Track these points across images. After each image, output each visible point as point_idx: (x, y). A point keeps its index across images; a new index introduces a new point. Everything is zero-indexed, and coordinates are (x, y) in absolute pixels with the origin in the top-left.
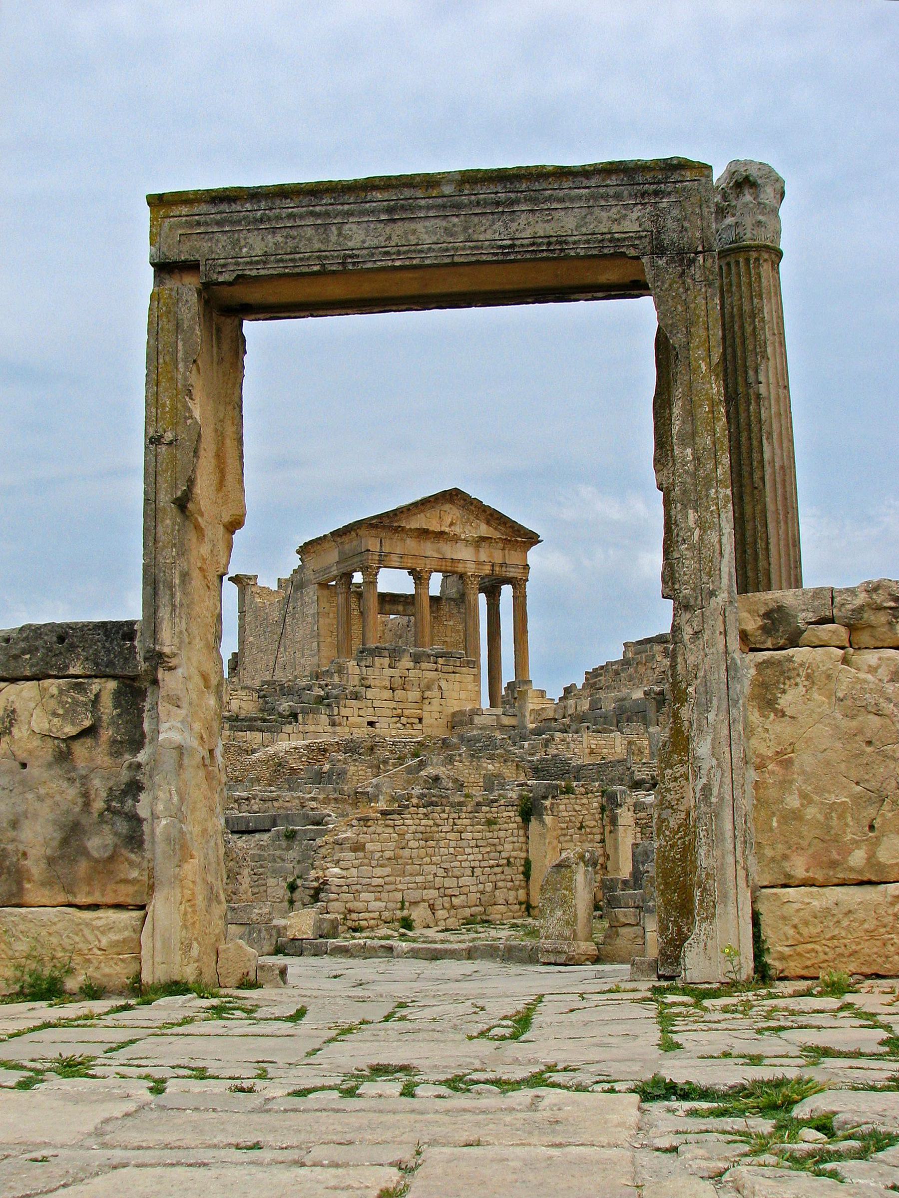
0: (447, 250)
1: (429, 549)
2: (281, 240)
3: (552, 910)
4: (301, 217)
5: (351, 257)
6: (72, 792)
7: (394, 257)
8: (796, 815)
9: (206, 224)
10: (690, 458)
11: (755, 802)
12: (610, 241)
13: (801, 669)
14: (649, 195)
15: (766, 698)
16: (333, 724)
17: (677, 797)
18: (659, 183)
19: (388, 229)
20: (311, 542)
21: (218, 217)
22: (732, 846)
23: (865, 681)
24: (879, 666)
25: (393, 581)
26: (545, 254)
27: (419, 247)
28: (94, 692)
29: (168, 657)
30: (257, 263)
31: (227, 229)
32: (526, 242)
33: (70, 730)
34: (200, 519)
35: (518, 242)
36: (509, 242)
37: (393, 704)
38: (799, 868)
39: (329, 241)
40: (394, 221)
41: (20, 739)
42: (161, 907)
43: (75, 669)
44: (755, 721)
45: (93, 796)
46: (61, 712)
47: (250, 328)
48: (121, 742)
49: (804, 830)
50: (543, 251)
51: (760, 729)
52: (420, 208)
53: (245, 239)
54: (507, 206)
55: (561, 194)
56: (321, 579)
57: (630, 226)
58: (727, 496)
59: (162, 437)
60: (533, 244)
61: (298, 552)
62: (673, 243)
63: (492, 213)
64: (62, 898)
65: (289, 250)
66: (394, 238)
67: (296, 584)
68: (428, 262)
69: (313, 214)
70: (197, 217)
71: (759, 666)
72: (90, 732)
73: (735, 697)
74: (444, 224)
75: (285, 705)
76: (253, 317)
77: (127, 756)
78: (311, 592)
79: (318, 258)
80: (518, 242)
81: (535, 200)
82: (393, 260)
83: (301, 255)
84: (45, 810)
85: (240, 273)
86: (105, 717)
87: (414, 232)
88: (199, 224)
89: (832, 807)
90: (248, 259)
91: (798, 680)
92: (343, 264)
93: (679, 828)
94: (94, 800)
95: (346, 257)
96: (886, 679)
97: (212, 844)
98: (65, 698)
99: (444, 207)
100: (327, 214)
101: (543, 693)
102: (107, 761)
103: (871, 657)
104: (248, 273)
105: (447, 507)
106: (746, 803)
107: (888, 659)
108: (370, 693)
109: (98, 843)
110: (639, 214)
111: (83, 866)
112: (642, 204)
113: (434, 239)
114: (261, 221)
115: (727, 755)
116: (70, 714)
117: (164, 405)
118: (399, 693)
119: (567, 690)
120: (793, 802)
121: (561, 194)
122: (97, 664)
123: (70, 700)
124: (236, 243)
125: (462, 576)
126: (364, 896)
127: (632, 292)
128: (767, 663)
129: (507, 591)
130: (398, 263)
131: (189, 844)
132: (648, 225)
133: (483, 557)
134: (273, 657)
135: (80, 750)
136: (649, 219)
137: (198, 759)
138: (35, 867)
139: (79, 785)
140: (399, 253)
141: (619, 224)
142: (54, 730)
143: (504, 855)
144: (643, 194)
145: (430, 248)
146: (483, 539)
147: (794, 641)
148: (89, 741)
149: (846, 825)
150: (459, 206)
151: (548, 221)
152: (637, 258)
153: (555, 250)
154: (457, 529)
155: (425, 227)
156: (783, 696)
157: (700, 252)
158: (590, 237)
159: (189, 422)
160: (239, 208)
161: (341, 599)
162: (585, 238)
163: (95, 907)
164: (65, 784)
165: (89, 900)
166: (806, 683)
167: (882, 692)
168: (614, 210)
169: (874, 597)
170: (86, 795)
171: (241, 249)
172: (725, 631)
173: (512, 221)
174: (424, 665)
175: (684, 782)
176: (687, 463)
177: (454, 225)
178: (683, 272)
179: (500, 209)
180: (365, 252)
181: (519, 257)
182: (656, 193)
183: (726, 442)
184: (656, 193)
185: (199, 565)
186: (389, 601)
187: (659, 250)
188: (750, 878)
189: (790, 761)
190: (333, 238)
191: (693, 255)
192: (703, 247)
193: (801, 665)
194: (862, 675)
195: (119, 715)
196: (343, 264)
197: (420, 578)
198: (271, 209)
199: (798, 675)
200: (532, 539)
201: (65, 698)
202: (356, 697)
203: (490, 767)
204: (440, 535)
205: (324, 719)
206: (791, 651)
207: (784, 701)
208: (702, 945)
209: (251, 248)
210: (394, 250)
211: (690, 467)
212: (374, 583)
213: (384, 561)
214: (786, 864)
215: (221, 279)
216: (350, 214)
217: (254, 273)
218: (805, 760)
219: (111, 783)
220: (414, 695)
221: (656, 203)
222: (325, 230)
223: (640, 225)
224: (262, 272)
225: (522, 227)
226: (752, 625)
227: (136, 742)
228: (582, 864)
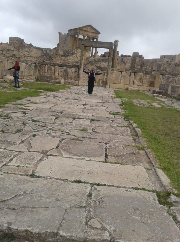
1: (86, 33)
6: (75, 74)
15: (112, 74)
16: (73, 57)
25: (81, 37)
38: (112, 83)
56: (71, 35)
61: (68, 31)
67: (68, 35)
75: (67, 54)
78: (69, 37)
101: (98, 55)
103: (117, 72)
105: (89, 27)
109: (76, 77)
111: (75, 78)
120: (112, 79)
125: (90, 37)
133: (93, 35)
134: (63, 45)
135: (76, 72)
146: (93, 32)
154: (90, 31)
161: (74, 38)
186: (80, 39)
197: (84, 37)
200: (99, 33)
202: (76, 54)
204: (87, 31)
212: (78, 37)
213: (80, 34)
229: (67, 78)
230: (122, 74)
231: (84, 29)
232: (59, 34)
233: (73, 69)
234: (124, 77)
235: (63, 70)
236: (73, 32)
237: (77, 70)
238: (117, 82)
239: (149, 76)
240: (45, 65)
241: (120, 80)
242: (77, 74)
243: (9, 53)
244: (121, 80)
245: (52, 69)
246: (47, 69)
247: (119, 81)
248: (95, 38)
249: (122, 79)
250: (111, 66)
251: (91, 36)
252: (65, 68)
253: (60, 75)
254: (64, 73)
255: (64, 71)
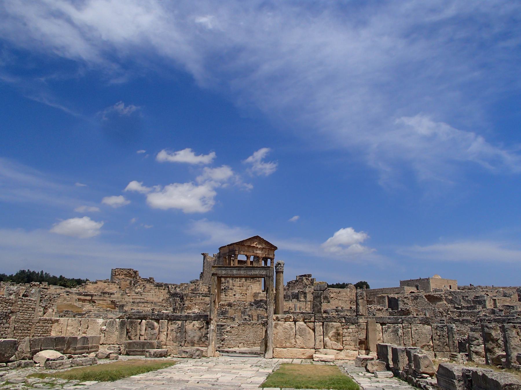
6: (200, 334)
15: (275, 327)
42: (210, 347)
57: (264, 273)
72: (203, 327)
84: (197, 336)
105: (255, 240)
106: (273, 339)
108: (234, 287)
109: (203, 339)
116: (201, 325)
125: (258, 257)
129: (269, 260)
138: (196, 342)
187: (267, 276)
197: (248, 257)
200: (276, 248)
202: (231, 289)
205: (224, 294)
218: (279, 334)
220: (245, 288)
226: (275, 318)
227: (208, 328)
229: (183, 344)
230: (297, 327)
231: (248, 243)
232: (203, 256)
233: (197, 324)
234: (301, 332)
235: (176, 326)
236: (227, 250)
238: (288, 344)
239: (354, 326)
240: (140, 320)
241: (294, 340)
242: (204, 333)
243: (105, 299)
244: (297, 340)
245: (153, 326)
246: (144, 328)
247: (293, 341)
248: (269, 258)
249: (297, 336)
252: (180, 322)
253: (170, 337)
254: (177, 333)
255: (178, 328)
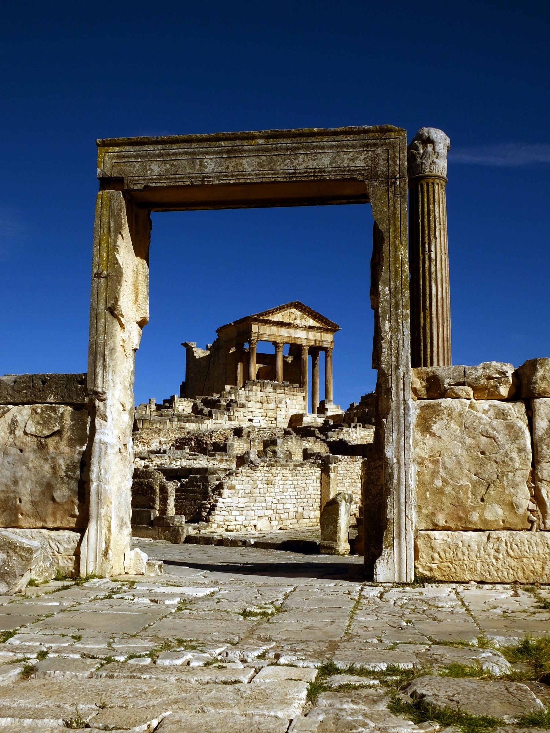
0: (259, 175)
2: (168, 167)
3: (328, 525)
4: (180, 154)
5: (207, 177)
6: (47, 467)
7: (230, 178)
8: (441, 491)
9: (128, 157)
10: (388, 292)
11: (417, 483)
12: (349, 171)
13: (445, 411)
14: (371, 146)
15: (425, 426)
16: (230, 420)
17: (377, 477)
18: (377, 139)
19: (227, 163)
20: (223, 327)
21: (135, 153)
22: (404, 507)
23: (481, 418)
24: (489, 410)
26: (312, 178)
27: (244, 173)
28: (61, 412)
29: (101, 394)
30: (156, 179)
31: (140, 160)
32: (302, 171)
33: (46, 432)
34: (122, 319)
35: (298, 171)
36: (292, 171)
37: (261, 410)
39: (195, 168)
40: (230, 158)
41: (19, 436)
43: (51, 399)
44: (418, 438)
45: (58, 469)
46: (42, 422)
47: (155, 216)
48: (74, 439)
49: (444, 499)
50: (311, 176)
51: (421, 443)
52: (245, 151)
53: (150, 166)
54: (292, 151)
55: (322, 144)
57: (360, 163)
58: (407, 314)
59: (101, 274)
60: (306, 172)
61: (216, 331)
62: (383, 173)
63: (284, 155)
64: (40, 524)
65: (173, 172)
66: (231, 167)
68: (248, 181)
69: (186, 153)
70: (123, 153)
71: (422, 408)
72: (59, 433)
73: (408, 425)
74: (258, 160)
76: (156, 209)
77: (78, 448)
79: (189, 177)
80: (298, 171)
81: (307, 148)
82: (230, 180)
83: (179, 176)
85: (146, 185)
86: (66, 426)
87: (241, 164)
88: (124, 157)
89: (461, 487)
90: (150, 177)
91: (443, 416)
92: (202, 181)
93: (377, 495)
94: (58, 471)
95: (204, 177)
96: (493, 417)
97: (124, 495)
98: (44, 415)
99: (258, 150)
100: (193, 153)
102: (66, 450)
104: (150, 185)
107: (494, 406)
108: (250, 404)
110: (365, 156)
112: (367, 151)
113: (252, 168)
114: (158, 156)
115: (403, 457)
117: (103, 257)
118: (265, 405)
119: (352, 405)
120: (438, 483)
121: (322, 144)
122: (62, 397)
123: (47, 416)
124: (144, 169)
126: (234, 513)
127: (362, 200)
128: (427, 407)
130: (232, 182)
131: (109, 496)
132: (369, 162)
135: (51, 443)
136: (370, 160)
137: (117, 449)
138: (26, 506)
139: (50, 463)
140: (233, 176)
141: (353, 162)
142: (38, 432)
143: (308, 493)
144: (367, 145)
145: (249, 174)
147: (444, 394)
148: (57, 438)
149: (468, 497)
150: (266, 150)
151: (315, 160)
152: (363, 181)
153: (318, 176)
154: (298, 322)
155: (247, 162)
156: (435, 425)
157: (398, 178)
158: (337, 169)
159: (116, 266)
160: (146, 149)
162: (335, 169)
163: (57, 529)
164: (42, 462)
165: (55, 526)
166: (448, 418)
167: (490, 424)
168: (351, 154)
169: (488, 371)
170: (53, 468)
171: (147, 172)
172: (404, 388)
173: (295, 159)
174: (278, 391)
175: (380, 470)
176: (386, 295)
177: (263, 161)
178: (388, 189)
179: (289, 153)
180: (213, 175)
181: (298, 179)
182: (375, 145)
183: (408, 284)
184: (375, 145)
185: (121, 344)
188: (414, 525)
189: (438, 461)
190: (197, 167)
191: (393, 180)
192: (400, 175)
193: (445, 408)
194: (479, 415)
195: (73, 425)
196: (202, 181)
198: (164, 150)
199: (444, 414)
201: (44, 415)
202: (243, 406)
203: (307, 445)
205: (226, 417)
206: (440, 400)
207: (435, 428)
208: (386, 561)
209: (153, 171)
210: (230, 174)
211: (387, 297)
214: (433, 518)
215: (135, 188)
216: (208, 153)
217: (153, 185)
219: (69, 462)
220: (272, 406)
221: (374, 150)
222: (193, 162)
223: (365, 163)
224: (158, 185)
225: (300, 162)
228: (344, 501)
232: (184, 349)
237: (68, 421)
238: (495, 512)
250: (406, 353)
251: (304, 343)
